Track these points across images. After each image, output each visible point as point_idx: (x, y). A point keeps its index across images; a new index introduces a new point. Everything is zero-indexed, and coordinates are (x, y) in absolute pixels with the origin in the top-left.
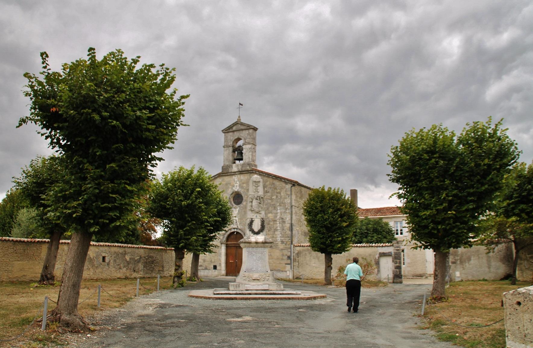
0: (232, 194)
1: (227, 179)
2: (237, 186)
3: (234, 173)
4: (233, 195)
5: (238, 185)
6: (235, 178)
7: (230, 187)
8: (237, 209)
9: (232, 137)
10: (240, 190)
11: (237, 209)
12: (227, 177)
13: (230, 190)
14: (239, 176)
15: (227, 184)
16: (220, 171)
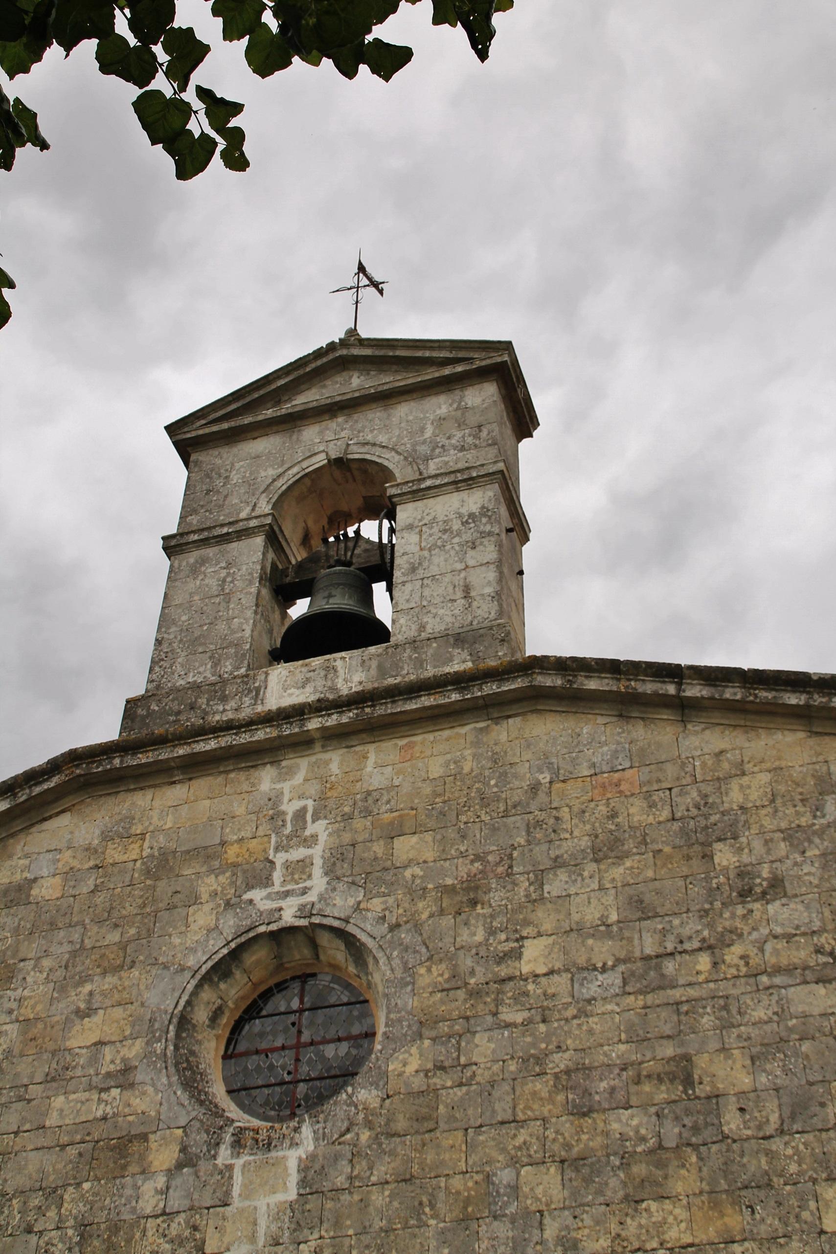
0: (221, 970)
1: (166, 811)
2: (303, 867)
3: (285, 737)
4: (235, 991)
5: (317, 853)
6: (288, 786)
7: (209, 884)
8: (292, 1159)
9: (264, 467)
10: (342, 904)
11: (292, 1159)
12: (177, 793)
13: (202, 917)
14: (335, 761)
15: (162, 865)
16: (105, 728)
